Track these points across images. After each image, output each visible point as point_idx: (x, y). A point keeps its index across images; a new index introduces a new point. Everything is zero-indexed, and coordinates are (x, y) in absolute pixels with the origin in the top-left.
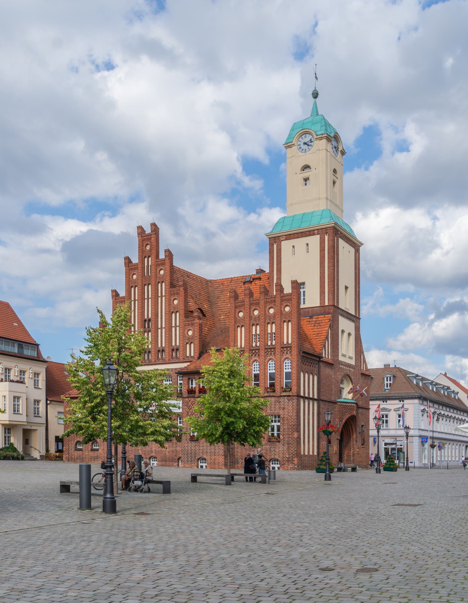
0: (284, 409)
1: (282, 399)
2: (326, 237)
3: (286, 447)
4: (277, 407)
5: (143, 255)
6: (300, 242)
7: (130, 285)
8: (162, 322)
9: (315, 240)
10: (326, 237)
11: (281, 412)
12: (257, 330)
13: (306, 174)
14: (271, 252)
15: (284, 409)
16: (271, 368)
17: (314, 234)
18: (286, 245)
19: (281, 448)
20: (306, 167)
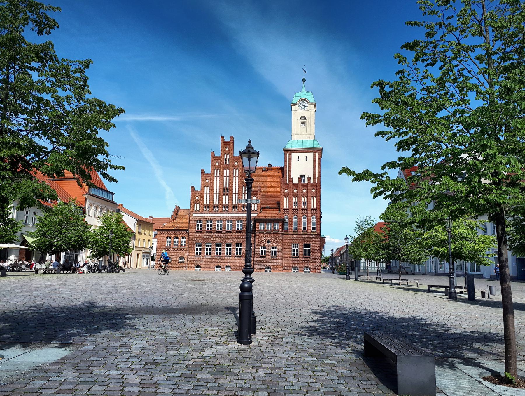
0: (313, 241)
1: (311, 236)
2: (317, 155)
3: (314, 261)
4: (309, 240)
5: (224, 152)
6: (302, 155)
7: (214, 168)
8: (235, 190)
9: (310, 155)
10: (317, 155)
11: (311, 242)
12: (295, 200)
13: (303, 120)
14: (286, 158)
15: (313, 241)
16: (304, 220)
17: (310, 152)
18: (294, 156)
19: (311, 261)
20: (303, 117)
